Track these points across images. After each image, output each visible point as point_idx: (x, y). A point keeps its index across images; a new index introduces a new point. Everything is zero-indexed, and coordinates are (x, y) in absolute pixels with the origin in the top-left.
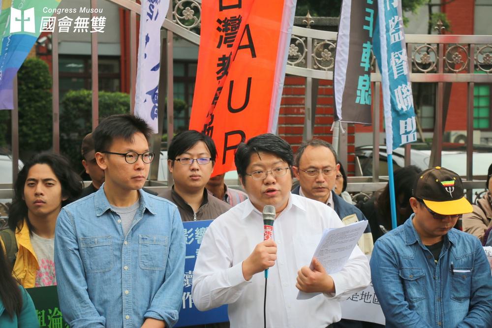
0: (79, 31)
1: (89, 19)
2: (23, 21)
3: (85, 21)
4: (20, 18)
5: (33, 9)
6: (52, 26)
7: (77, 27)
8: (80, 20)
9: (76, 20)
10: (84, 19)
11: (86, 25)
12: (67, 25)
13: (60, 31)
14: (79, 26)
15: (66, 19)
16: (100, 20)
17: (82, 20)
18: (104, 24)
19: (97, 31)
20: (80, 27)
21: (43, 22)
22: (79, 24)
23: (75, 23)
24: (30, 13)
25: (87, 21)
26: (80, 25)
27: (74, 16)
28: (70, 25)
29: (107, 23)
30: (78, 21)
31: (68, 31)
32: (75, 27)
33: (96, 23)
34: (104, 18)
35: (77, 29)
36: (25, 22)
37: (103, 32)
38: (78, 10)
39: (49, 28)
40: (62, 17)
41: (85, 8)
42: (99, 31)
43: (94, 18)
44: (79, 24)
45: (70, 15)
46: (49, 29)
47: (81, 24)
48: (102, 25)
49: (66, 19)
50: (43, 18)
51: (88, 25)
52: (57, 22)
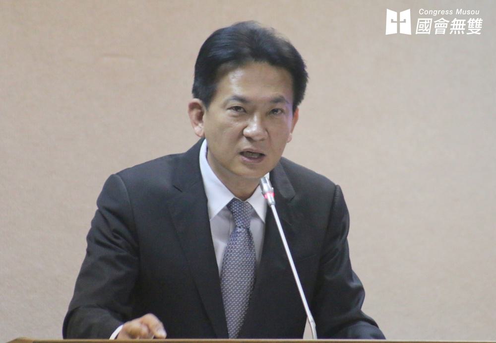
0: (455, 33)
1: (465, 20)
2: (398, 22)
3: (462, 23)
4: (395, 20)
5: (409, 10)
6: (429, 28)
7: (453, 29)
8: (456, 23)
9: (452, 22)
10: (460, 21)
11: (463, 27)
12: (444, 27)
13: (436, 33)
14: (455, 27)
15: (442, 20)
16: (476, 21)
17: (459, 22)
18: (480, 26)
19: (473, 32)
20: (456, 29)
21: (419, 24)
22: (455, 26)
23: (451, 25)
24: (406, 14)
25: (463, 23)
26: (457, 27)
27: (450, 18)
28: (446, 27)
29: (483, 24)
30: (454, 23)
31: (444, 33)
32: (451, 29)
33: (472, 25)
34: (481, 20)
35: (454, 31)
36: (401, 24)
37: (479, 34)
38: (454, 12)
39: (426, 29)
40: (438, 19)
41: (461, 10)
42: (476, 33)
43: (470, 20)
44: (455, 26)
45: (446, 17)
46: (425, 31)
47: (458, 25)
49: (442, 20)
50: (419, 19)
51: (464, 27)
52: (433, 24)
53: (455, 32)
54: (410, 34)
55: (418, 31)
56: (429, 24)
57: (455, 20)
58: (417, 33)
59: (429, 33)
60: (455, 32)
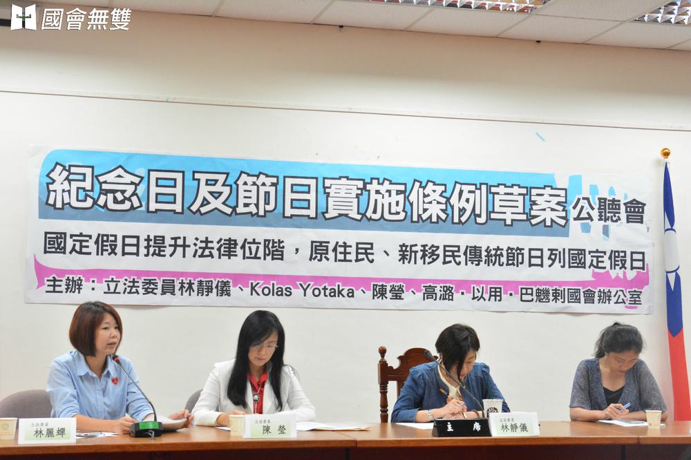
1: (107, 11)
10: (101, 12)
11: (104, 20)
12: (79, 20)
13: (69, 28)
16: (123, 13)
19: (119, 27)
20: (96, 23)
23: (89, 17)
26: (96, 20)
28: (82, 20)
33: (117, 18)
35: (92, 25)
37: (127, 29)
39: (55, 23)
42: (122, 27)
48: (126, 20)
50: (46, 10)
53: (94, 26)
54: (35, 28)
55: (45, 26)
56: (60, 16)
57: (94, 11)
58: (43, 28)
59: (59, 28)
60: (94, 26)
